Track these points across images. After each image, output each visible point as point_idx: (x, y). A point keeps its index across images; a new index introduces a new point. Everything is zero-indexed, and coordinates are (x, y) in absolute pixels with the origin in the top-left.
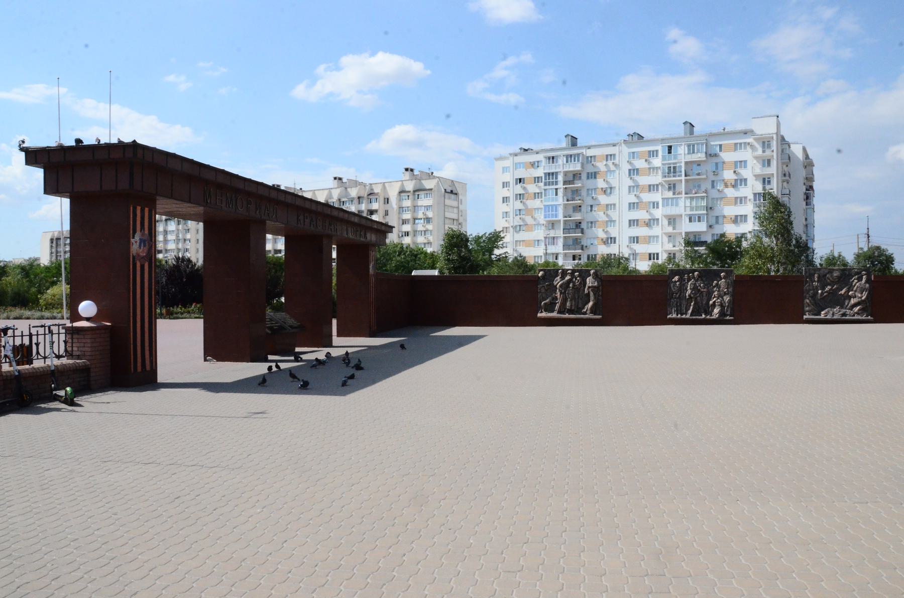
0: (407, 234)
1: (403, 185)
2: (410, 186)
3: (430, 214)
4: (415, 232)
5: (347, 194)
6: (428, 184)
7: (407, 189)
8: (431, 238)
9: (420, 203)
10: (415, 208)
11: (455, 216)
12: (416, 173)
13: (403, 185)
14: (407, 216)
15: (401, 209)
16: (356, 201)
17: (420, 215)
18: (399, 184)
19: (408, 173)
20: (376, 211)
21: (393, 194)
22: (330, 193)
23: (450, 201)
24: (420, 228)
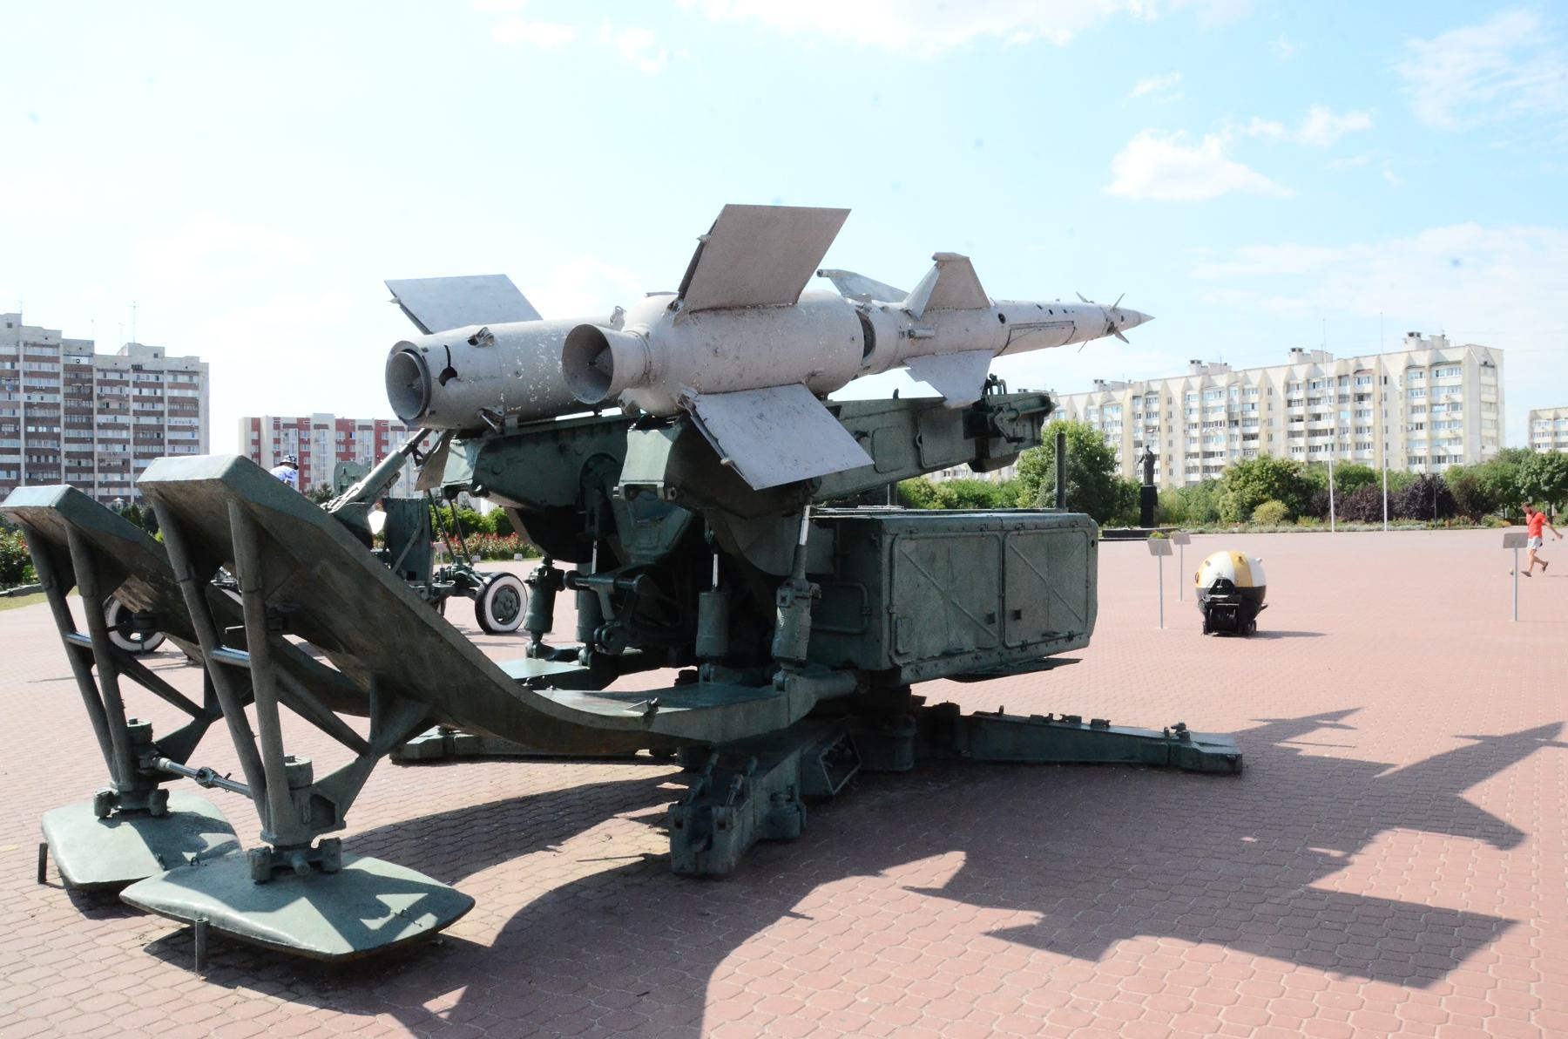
0: (1420, 426)
1: (1410, 358)
2: (1423, 359)
3: (1458, 398)
4: (1435, 424)
5: (1318, 373)
6: (1449, 356)
7: (1418, 363)
8: (1460, 432)
9: (1442, 381)
10: (1433, 389)
11: (1492, 399)
12: (1423, 337)
13: (1410, 358)
14: (1420, 401)
15: (1411, 392)
16: (1336, 382)
17: (1443, 400)
18: (1405, 356)
19: (1413, 341)
20: (1369, 395)
21: (1396, 369)
22: (1291, 371)
23: (1487, 378)
24: (1442, 417)
